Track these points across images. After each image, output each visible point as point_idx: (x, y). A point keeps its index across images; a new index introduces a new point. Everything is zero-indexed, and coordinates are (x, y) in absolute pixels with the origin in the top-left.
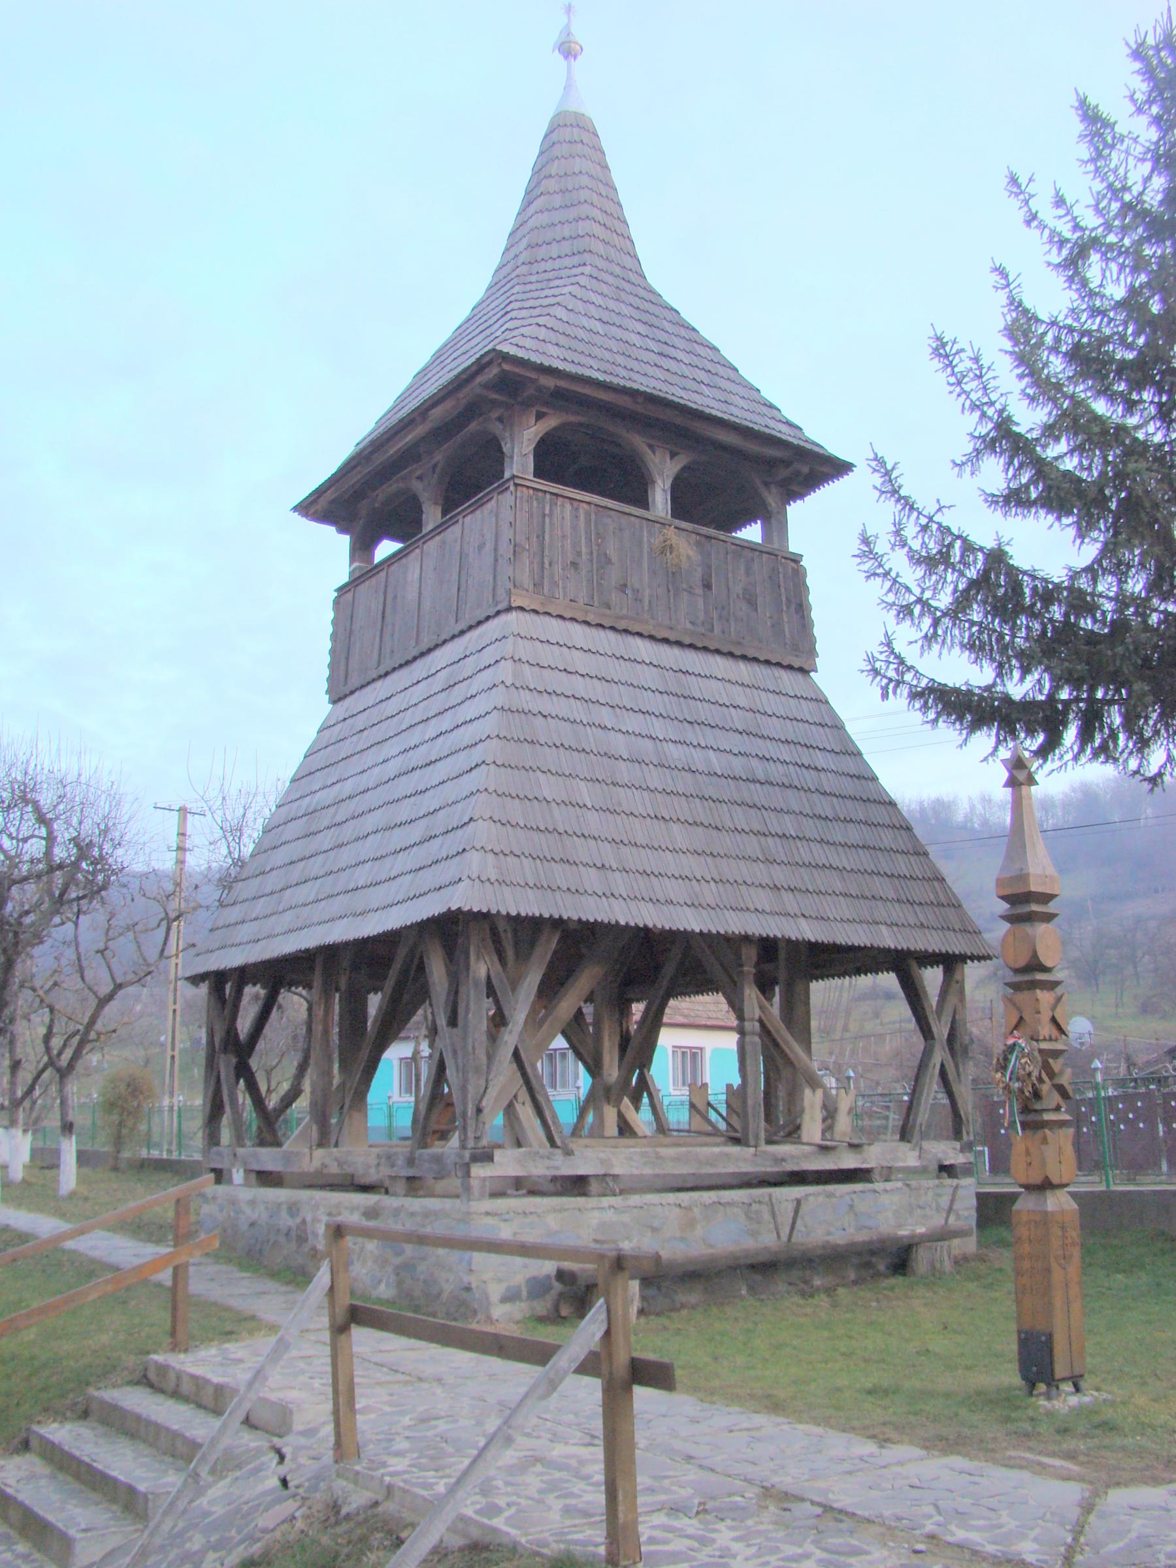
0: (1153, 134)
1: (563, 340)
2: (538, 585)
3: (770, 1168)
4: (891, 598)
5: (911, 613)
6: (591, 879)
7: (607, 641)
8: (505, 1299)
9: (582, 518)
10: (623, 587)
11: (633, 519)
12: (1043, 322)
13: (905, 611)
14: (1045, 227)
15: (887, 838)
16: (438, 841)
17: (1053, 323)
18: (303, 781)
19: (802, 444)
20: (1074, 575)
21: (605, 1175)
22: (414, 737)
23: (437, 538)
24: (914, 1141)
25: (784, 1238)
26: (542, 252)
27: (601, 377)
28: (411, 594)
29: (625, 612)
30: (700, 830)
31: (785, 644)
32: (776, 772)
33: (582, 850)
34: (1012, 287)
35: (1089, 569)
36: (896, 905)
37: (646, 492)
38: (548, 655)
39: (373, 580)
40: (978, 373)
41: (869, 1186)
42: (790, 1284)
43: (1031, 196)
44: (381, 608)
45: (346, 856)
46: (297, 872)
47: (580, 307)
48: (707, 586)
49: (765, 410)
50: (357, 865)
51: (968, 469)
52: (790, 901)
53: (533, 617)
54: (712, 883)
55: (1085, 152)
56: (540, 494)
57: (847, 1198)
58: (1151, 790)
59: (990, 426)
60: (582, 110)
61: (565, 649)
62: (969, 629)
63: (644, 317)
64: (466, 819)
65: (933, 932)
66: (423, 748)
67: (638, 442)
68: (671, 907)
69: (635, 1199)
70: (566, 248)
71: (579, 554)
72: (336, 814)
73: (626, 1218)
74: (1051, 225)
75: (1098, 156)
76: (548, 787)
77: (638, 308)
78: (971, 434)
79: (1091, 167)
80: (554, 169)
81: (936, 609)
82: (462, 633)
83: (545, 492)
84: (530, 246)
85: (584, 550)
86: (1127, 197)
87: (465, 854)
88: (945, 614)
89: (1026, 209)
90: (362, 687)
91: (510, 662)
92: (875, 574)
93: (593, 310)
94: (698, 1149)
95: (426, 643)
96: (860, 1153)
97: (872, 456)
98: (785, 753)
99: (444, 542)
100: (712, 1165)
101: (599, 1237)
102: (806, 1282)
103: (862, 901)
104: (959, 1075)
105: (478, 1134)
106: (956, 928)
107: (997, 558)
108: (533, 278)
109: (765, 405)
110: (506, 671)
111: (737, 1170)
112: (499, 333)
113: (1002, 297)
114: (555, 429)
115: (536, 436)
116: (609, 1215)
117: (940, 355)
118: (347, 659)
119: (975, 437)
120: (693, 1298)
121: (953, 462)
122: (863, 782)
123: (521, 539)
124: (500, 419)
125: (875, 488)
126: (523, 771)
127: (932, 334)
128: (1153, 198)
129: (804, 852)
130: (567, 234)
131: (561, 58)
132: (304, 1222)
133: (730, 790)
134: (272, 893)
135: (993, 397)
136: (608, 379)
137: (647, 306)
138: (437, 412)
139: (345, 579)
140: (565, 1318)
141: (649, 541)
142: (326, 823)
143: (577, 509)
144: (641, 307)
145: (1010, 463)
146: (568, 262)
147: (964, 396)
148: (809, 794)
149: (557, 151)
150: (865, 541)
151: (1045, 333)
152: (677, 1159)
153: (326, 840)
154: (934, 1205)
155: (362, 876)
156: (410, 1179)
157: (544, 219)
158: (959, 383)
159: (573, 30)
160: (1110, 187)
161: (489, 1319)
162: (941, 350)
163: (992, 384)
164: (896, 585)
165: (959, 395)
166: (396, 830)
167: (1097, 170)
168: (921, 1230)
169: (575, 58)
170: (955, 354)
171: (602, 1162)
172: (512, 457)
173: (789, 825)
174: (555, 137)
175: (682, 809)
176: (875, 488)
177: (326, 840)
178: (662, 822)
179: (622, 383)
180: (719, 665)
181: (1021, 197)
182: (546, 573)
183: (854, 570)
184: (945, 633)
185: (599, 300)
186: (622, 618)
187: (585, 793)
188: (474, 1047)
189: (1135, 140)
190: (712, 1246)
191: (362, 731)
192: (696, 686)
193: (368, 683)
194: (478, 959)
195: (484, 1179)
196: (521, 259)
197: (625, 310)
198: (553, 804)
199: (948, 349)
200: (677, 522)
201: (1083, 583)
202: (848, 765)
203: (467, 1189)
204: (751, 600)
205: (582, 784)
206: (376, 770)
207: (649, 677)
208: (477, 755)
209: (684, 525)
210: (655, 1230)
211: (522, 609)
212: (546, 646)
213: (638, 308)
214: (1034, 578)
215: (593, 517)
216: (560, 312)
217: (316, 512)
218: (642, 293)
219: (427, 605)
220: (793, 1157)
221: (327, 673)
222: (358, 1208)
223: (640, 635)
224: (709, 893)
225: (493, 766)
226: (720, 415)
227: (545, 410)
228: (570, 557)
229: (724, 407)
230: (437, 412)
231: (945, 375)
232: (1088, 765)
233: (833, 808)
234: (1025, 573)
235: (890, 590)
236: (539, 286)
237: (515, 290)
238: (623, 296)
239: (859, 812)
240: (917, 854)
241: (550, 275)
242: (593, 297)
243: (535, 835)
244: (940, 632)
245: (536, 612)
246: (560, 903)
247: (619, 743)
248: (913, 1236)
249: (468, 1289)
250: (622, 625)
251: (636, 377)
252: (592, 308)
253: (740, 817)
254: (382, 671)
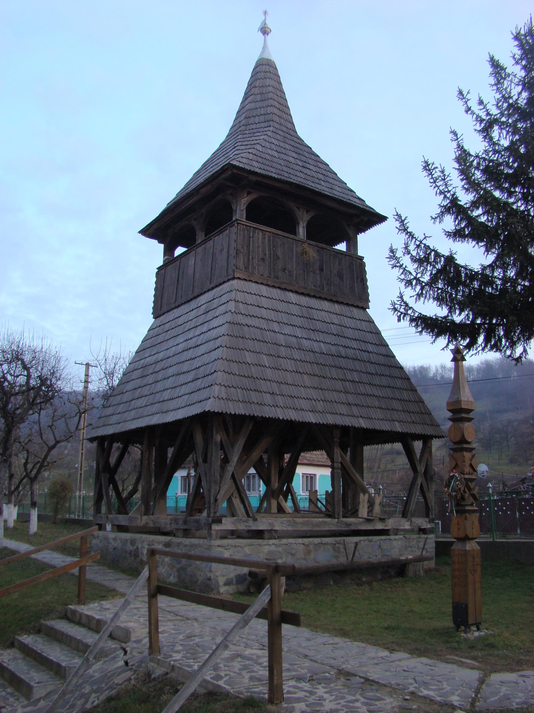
0: (523, 74)
1: (259, 160)
2: (247, 268)
3: (344, 529)
4: (403, 277)
5: (411, 284)
6: (268, 399)
7: (276, 293)
8: (226, 584)
9: (267, 239)
10: (284, 270)
11: (289, 239)
12: (472, 156)
13: (409, 283)
14: (474, 114)
15: (399, 383)
16: (201, 380)
17: (477, 156)
18: (141, 352)
19: (365, 208)
20: (484, 268)
21: (271, 530)
22: (190, 335)
23: (203, 246)
24: (408, 518)
25: (350, 559)
26: (251, 120)
27: (276, 176)
28: (191, 271)
29: (285, 280)
30: (316, 378)
31: (356, 296)
32: (350, 353)
33: (264, 386)
34: (459, 140)
35: (490, 266)
36: (402, 413)
37: (295, 228)
38: (251, 299)
39: (174, 264)
40: (443, 178)
41: (388, 537)
42: (352, 580)
43: (468, 100)
44: (177, 277)
45: (159, 386)
46: (138, 393)
47: (268, 145)
48: (321, 270)
49: (349, 192)
50: (164, 390)
51: (438, 220)
52: (355, 410)
53: (244, 282)
54: (321, 402)
55: (492, 81)
56: (248, 228)
57: (378, 542)
58: (516, 364)
59: (448, 201)
60: (270, 58)
61: (258, 297)
62: (437, 291)
63: (296, 150)
64: (213, 371)
65: (418, 425)
66: (194, 339)
67: (293, 206)
68: (303, 412)
69: (284, 541)
70: (262, 118)
71: (265, 254)
72: (155, 368)
73: (280, 549)
74: (477, 113)
75: (498, 83)
76: (249, 358)
77: (293, 146)
78: (439, 205)
79: (495, 88)
80: (257, 83)
81: (423, 282)
82: (213, 288)
83: (251, 227)
84: (246, 118)
85: (267, 253)
86: (511, 101)
87: (213, 387)
88: (426, 284)
89: (466, 105)
90: (168, 311)
91: (233, 302)
92: (396, 266)
93: (273, 146)
94: (313, 519)
95: (196, 293)
96: (384, 522)
97: (395, 214)
98: (354, 344)
99: (205, 248)
100: (318, 527)
101: (268, 557)
102: (359, 579)
103: (387, 411)
104: (428, 489)
105: (216, 511)
106: (429, 423)
107: (450, 260)
108: (247, 132)
109: (349, 190)
110: (231, 306)
111: (329, 529)
112: (231, 156)
113: (455, 144)
114: (256, 199)
115: (247, 202)
116: (273, 548)
117: (427, 170)
118: (162, 299)
119: (441, 206)
120: (309, 585)
121: (432, 217)
122: (389, 358)
123: (239, 247)
124: (231, 194)
125: (397, 228)
126: (238, 350)
127: (423, 160)
128: (522, 102)
129: (362, 389)
130: (262, 113)
131: (261, 34)
132: (137, 548)
133: (330, 361)
134: (126, 402)
135: (450, 188)
136: (280, 177)
137: (297, 145)
138: (203, 190)
139: (161, 263)
140: (252, 593)
141: (296, 249)
142: (151, 371)
143: (265, 235)
144: (295, 146)
145: (456, 218)
146: (262, 125)
147: (437, 188)
148: (364, 363)
149: (259, 76)
150: (392, 251)
151: (473, 161)
152: (303, 524)
153: (150, 379)
154: (416, 546)
155: (166, 395)
156: (185, 530)
157: (253, 105)
158: (435, 182)
159: (267, 22)
160: (503, 96)
161: (219, 593)
162: (427, 167)
163: (450, 183)
164: (405, 271)
165: (435, 188)
166: (182, 375)
167: (498, 89)
168: (410, 557)
169: (268, 35)
170: (433, 169)
171: (270, 524)
172: (236, 211)
173: (356, 376)
174: (258, 70)
175: (308, 368)
176: (397, 228)
177: (150, 379)
178: (299, 374)
179: (286, 179)
180: (326, 305)
181: (464, 100)
182: (250, 263)
183: (386, 264)
184: (426, 293)
185: (276, 142)
186: (283, 283)
187: (265, 360)
188: (214, 472)
189: (515, 76)
190: (318, 562)
191: (167, 331)
192: (315, 314)
193: (171, 310)
194: (217, 433)
195: (218, 531)
196: (242, 124)
197: (287, 147)
198: (251, 365)
199: (430, 167)
200: (309, 241)
201: (488, 272)
202: (383, 350)
203: (210, 535)
204: (341, 277)
205: (264, 356)
206: (174, 349)
207: (295, 310)
208: (218, 342)
209: (312, 242)
210: (292, 555)
211: (239, 278)
212: (250, 295)
213: (293, 146)
214: (466, 269)
215: (272, 238)
216: (259, 147)
217: (149, 234)
218: (295, 139)
219: (197, 275)
220: (354, 523)
221: (152, 305)
222: (161, 542)
223: (291, 291)
224: (320, 406)
225: (225, 348)
226: (328, 194)
227: (251, 190)
228: (261, 256)
229: (330, 191)
230: (203, 190)
231: (428, 178)
232: (488, 352)
233: (375, 369)
234: (462, 267)
235: (402, 273)
236: (250, 135)
237: (239, 137)
238: (287, 140)
239: (387, 371)
240: (412, 390)
241: (255, 131)
242: (273, 141)
243: (243, 378)
244: (424, 292)
245: (245, 280)
246: (254, 409)
247: (281, 339)
248: (407, 560)
249: (210, 579)
250: (283, 286)
251: (292, 176)
252: (273, 146)
253: (334, 373)
254: (177, 304)
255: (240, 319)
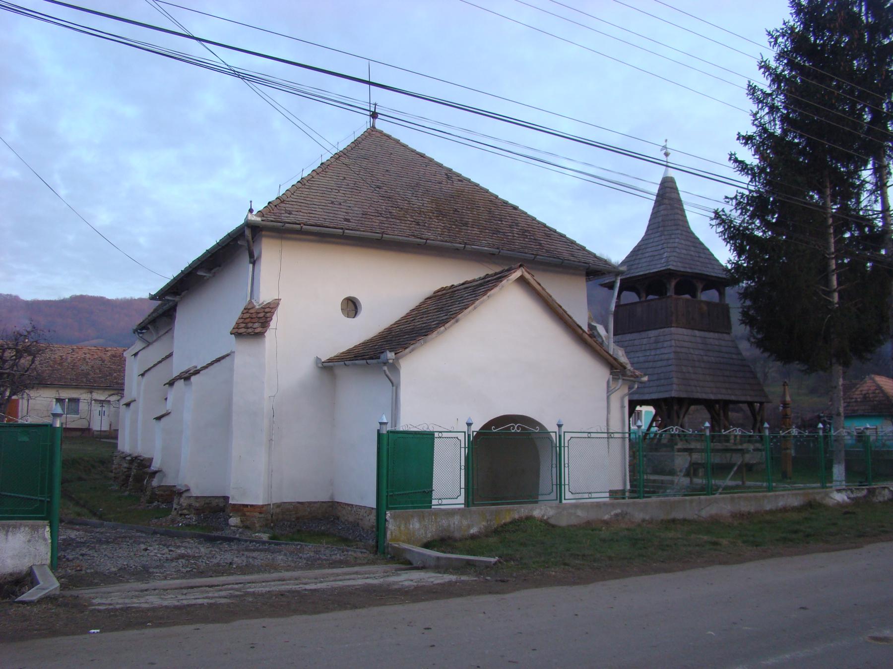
7: (689, 332)
76: (684, 369)
98: (726, 356)
255: (678, 350)
